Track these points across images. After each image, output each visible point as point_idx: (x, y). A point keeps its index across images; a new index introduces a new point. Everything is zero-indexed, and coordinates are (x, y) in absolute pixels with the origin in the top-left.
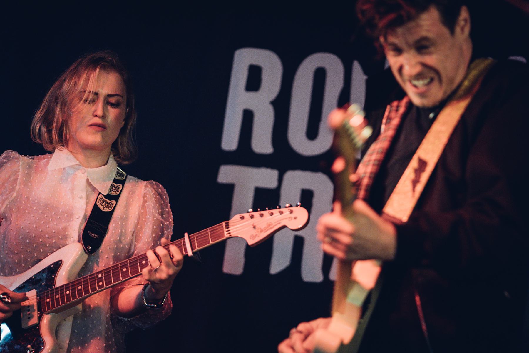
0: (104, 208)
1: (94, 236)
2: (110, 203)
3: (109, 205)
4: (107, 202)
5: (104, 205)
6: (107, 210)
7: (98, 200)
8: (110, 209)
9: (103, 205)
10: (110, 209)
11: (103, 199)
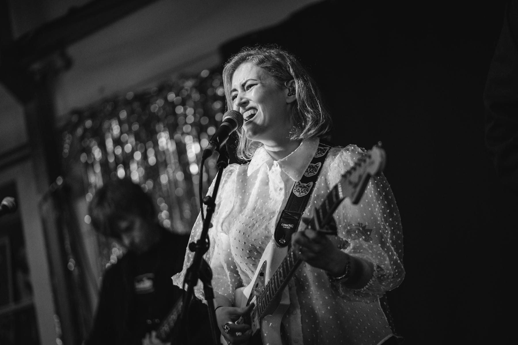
2: (307, 187)
3: (306, 189)
4: (304, 186)
6: (303, 194)
8: (306, 193)
9: (299, 192)
10: (306, 193)
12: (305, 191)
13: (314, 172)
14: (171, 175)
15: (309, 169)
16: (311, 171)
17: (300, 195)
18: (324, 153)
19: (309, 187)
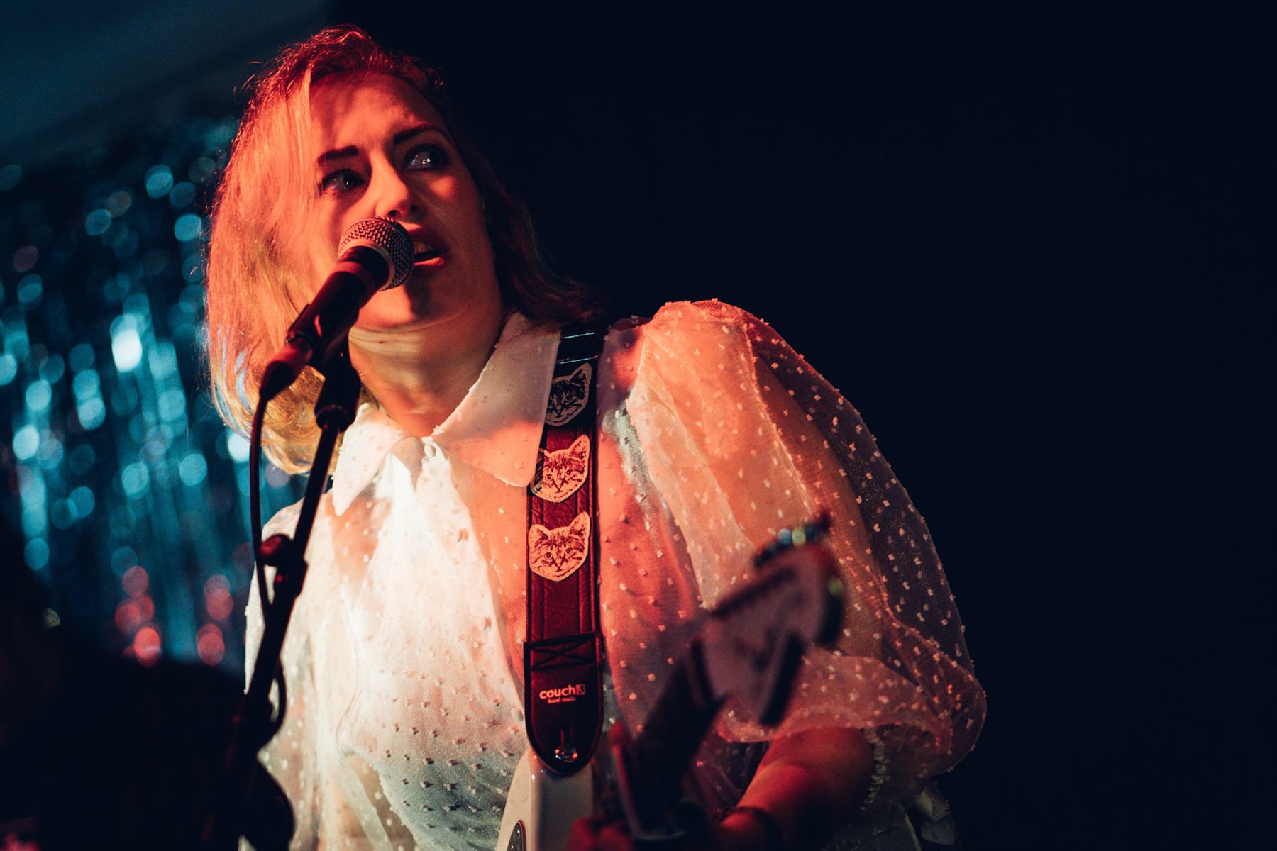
0: (559, 568)
1: (569, 696)
3: (573, 545)
4: (563, 538)
5: (555, 557)
6: (573, 565)
7: (533, 556)
9: (554, 562)
10: (579, 559)
11: (544, 537)
12: (575, 554)
13: (575, 554)
14: (161, 465)
15: (555, 401)
16: (563, 402)
17: (561, 573)
18: (582, 397)
19: (580, 533)
